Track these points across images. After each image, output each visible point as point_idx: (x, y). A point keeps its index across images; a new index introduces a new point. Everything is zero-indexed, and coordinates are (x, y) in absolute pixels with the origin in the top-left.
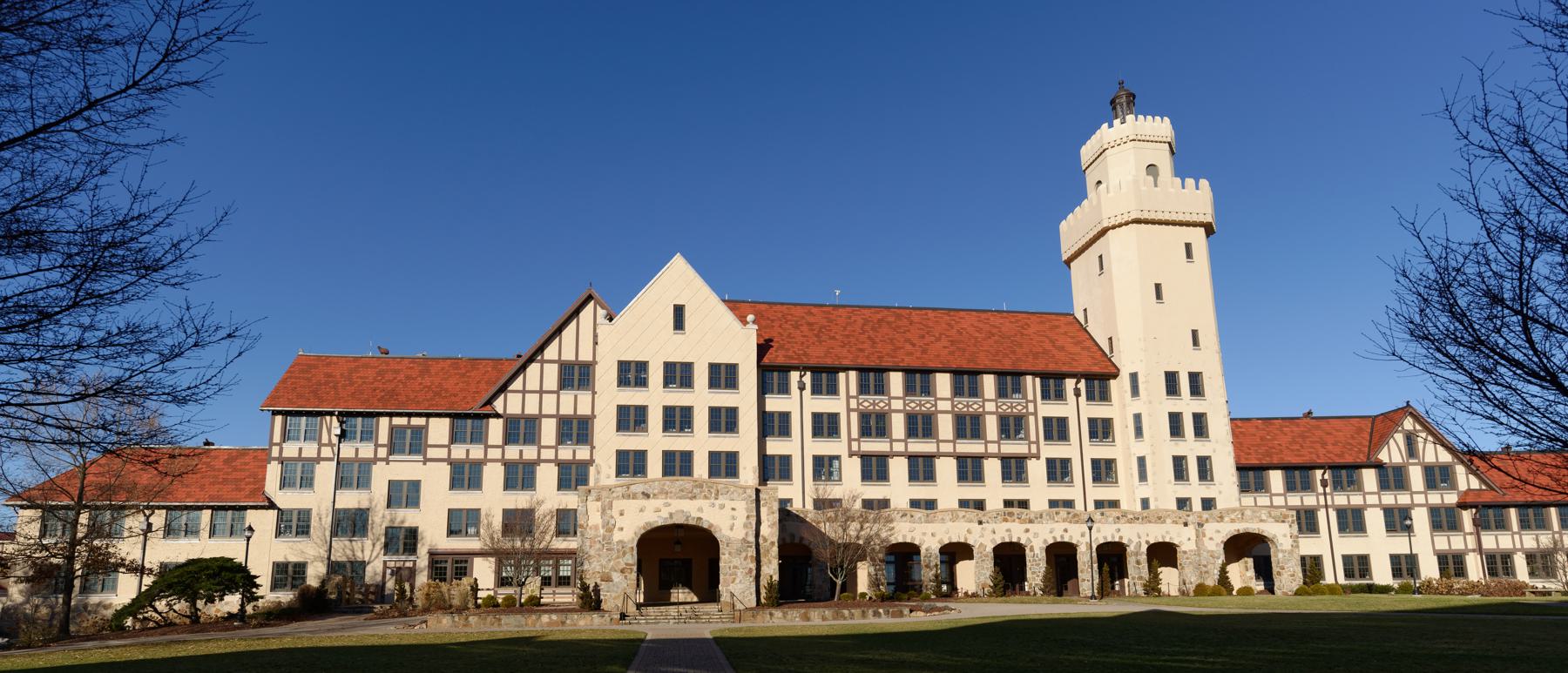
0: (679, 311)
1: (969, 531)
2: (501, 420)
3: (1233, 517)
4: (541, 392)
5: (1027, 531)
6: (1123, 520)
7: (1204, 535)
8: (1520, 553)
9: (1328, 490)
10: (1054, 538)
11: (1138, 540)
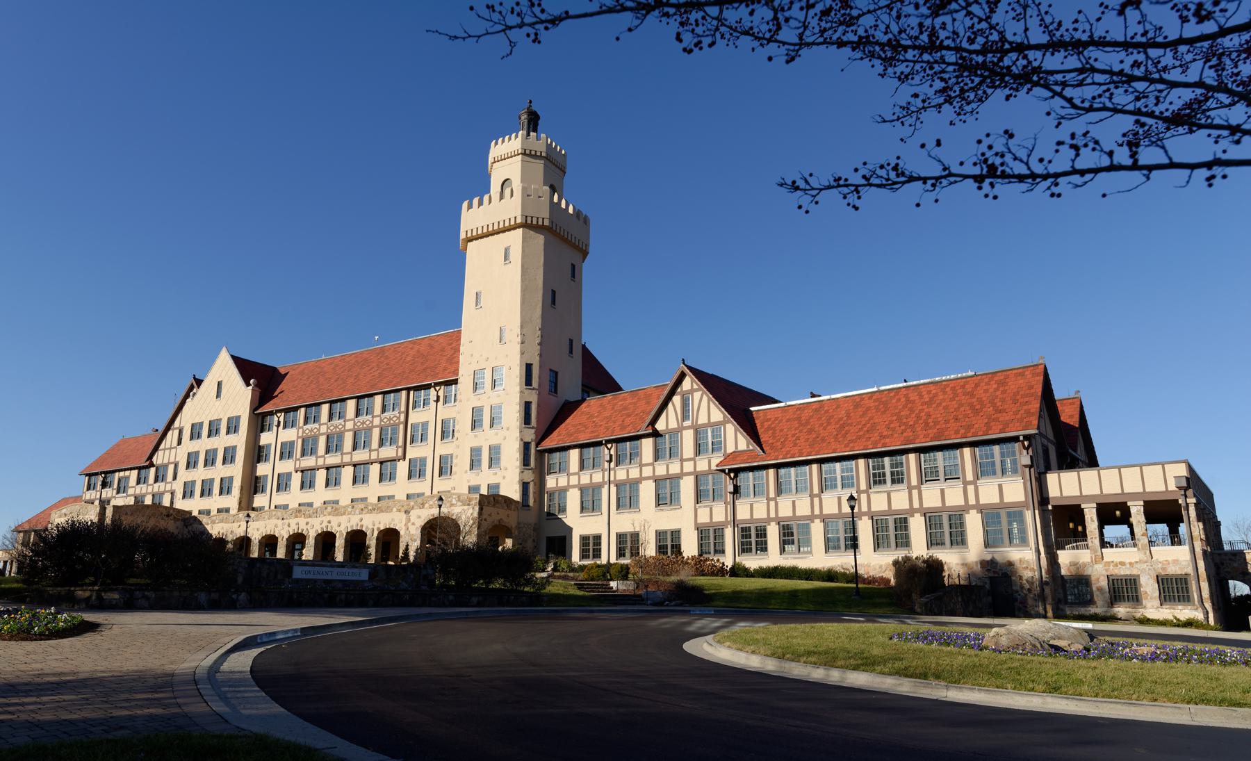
0: (219, 384)
3: (431, 503)
4: (171, 448)
5: (307, 524)
6: (364, 512)
7: (409, 520)
8: (773, 524)
9: (612, 464)
10: (322, 528)
11: (372, 527)
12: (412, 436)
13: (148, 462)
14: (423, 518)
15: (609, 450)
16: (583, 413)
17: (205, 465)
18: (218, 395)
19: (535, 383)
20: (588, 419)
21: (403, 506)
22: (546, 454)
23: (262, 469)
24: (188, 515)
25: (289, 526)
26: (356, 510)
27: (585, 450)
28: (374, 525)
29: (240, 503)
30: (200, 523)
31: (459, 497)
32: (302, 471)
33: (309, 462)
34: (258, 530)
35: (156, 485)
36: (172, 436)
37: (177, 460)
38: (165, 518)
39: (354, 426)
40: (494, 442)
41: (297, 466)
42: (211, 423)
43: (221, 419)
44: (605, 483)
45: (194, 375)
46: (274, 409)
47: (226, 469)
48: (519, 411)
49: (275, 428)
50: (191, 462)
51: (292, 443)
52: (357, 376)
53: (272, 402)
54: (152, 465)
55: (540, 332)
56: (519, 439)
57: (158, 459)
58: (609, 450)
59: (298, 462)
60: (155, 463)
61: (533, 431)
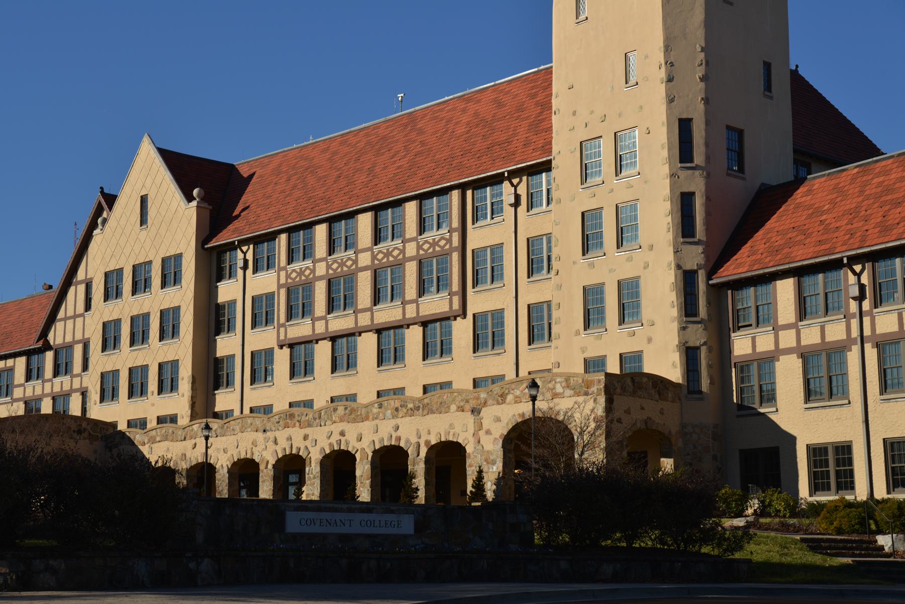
1: (254, 444)
2: (52, 351)
3: (518, 393)
4: (75, 317)
5: (306, 438)
7: (480, 426)
9: (866, 305)
10: (331, 445)
12: (476, 273)
13: (41, 343)
14: (505, 420)
15: (859, 275)
16: (798, 206)
17: (132, 343)
18: (143, 221)
19: (699, 158)
20: (810, 216)
21: (467, 401)
22: (729, 292)
23: (226, 345)
24: (111, 431)
25: (276, 442)
26: (387, 409)
27: (808, 280)
28: (420, 438)
29: (193, 406)
30: (131, 442)
31: (567, 380)
32: (291, 346)
33: (301, 329)
34: (225, 451)
35: (57, 380)
36: (75, 296)
37: (86, 337)
38: (75, 435)
39: (373, 261)
40: (627, 273)
41: (282, 337)
42: (135, 268)
43: (150, 262)
44: (854, 341)
45: (102, 188)
46: (236, 239)
47: (166, 348)
48: (671, 213)
49: (240, 272)
50: (110, 340)
51: (270, 297)
52: (371, 170)
53: (231, 227)
54: (47, 347)
55: (702, 55)
56: (673, 266)
57: (57, 336)
58: (859, 275)
59: (282, 330)
60: (52, 343)
61: (700, 249)
